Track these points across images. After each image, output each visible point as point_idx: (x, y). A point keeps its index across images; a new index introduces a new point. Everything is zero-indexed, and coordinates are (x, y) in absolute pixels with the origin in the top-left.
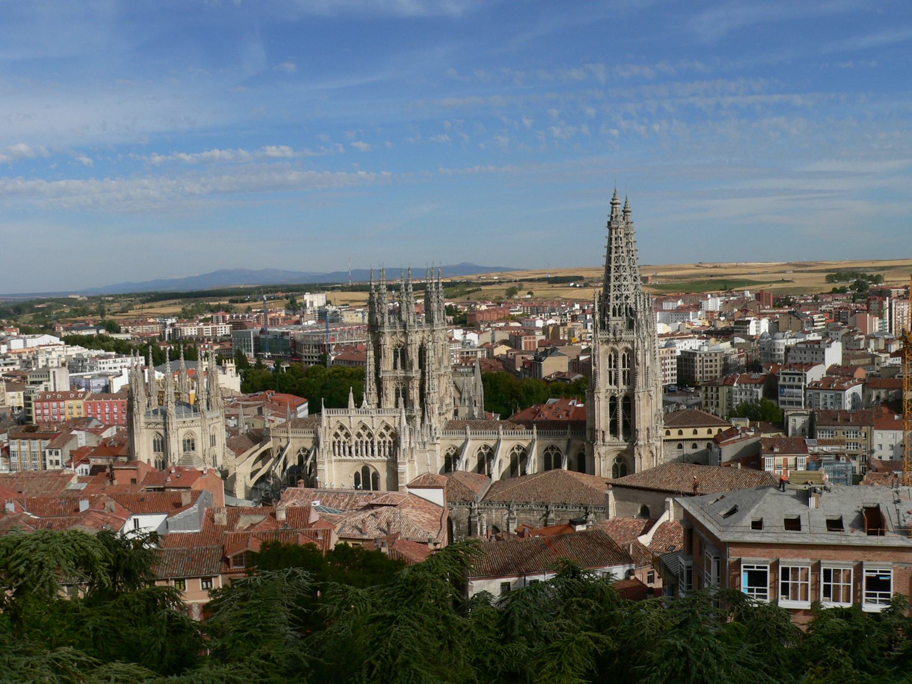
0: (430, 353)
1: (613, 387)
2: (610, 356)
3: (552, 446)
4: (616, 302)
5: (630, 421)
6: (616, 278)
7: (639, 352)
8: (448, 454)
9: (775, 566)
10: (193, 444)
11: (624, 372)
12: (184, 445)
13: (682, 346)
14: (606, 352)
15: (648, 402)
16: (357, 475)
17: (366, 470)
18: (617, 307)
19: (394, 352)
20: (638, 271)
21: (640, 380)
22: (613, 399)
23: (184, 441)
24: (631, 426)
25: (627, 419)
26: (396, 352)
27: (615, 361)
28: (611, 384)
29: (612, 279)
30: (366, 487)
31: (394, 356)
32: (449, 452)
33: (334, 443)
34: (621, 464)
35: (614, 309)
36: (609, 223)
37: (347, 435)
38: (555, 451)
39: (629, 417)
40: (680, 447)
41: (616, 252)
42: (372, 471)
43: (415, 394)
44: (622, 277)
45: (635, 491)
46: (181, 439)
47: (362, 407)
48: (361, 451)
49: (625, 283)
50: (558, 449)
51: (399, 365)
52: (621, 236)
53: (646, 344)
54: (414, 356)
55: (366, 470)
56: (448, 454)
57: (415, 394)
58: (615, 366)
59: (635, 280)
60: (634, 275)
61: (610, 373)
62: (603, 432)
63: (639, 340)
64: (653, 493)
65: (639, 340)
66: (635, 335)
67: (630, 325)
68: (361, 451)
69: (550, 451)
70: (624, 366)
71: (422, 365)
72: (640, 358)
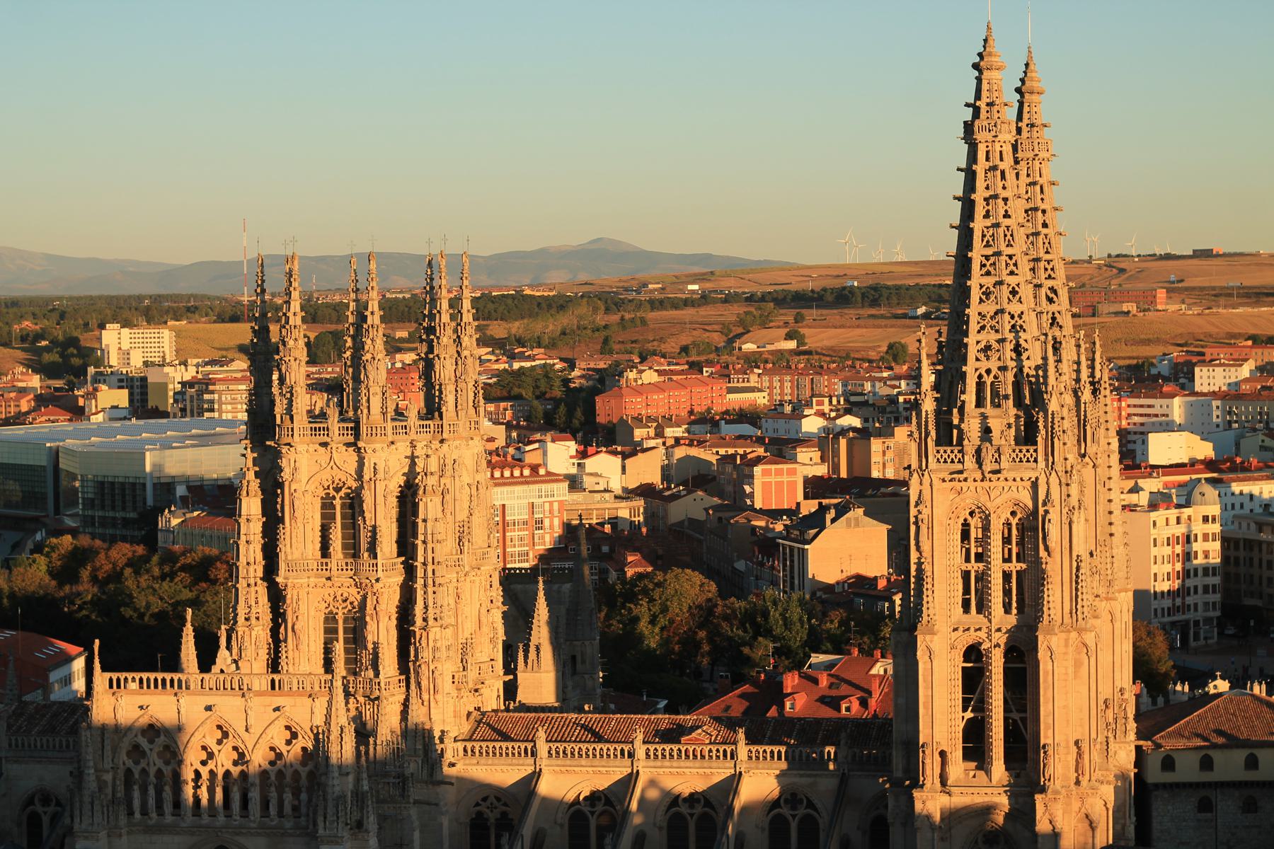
0: (429, 507)
1: (974, 617)
4: (984, 365)
5: (1024, 720)
6: (987, 294)
7: (1054, 515)
8: (480, 814)
11: (1007, 576)
13: (531, 501)
15: (1078, 664)
18: (988, 380)
19: (324, 506)
20: (1061, 273)
21: (1055, 597)
22: (973, 653)
24: (1028, 737)
25: (1016, 716)
26: (327, 505)
31: (323, 516)
32: (483, 808)
35: (980, 385)
36: (969, 128)
40: (1205, 806)
41: (987, 216)
43: (383, 632)
44: (1005, 291)
47: (215, 669)
49: (1015, 308)
52: (1002, 166)
53: (1074, 490)
57: (383, 632)
59: (1050, 300)
60: (1050, 283)
61: (966, 575)
62: (943, 754)
63: (1054, 479)
65: (1054, 479)
66: (1042, 464)
67: (1027, 436)
71: (406, 546)
72: (1054, 531)
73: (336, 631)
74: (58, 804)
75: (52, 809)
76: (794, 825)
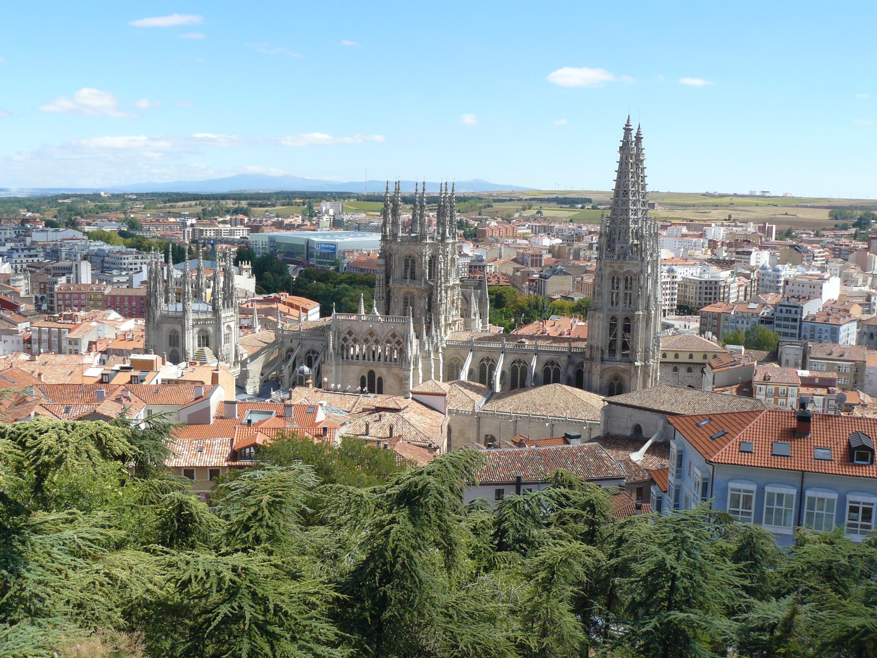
2: (613, 278)
9: (761, 491)
10: (207, 341)
11: (626, 294)
12: (199, 341)
14: (610, 274)
16: (363, 378)
17: (371, 374)
23: (199, 337)
25: (626, 340)
27: (618, 283)
28: (612, 305)
29: (620, 203)
30: (371, 391)
33: (343, 345)
38: (555, 367)
40: (675, 369)
42: (377, 377)
48: (368, 356)
50: (558, 365)
51: (408, 276)
55: (371, 374)
58: (618, 288)
64: (647, 412)
68: (368, 356)
70: (626, 288)
73: (407, 302)
74: (318, 354)
75: (315, 355)
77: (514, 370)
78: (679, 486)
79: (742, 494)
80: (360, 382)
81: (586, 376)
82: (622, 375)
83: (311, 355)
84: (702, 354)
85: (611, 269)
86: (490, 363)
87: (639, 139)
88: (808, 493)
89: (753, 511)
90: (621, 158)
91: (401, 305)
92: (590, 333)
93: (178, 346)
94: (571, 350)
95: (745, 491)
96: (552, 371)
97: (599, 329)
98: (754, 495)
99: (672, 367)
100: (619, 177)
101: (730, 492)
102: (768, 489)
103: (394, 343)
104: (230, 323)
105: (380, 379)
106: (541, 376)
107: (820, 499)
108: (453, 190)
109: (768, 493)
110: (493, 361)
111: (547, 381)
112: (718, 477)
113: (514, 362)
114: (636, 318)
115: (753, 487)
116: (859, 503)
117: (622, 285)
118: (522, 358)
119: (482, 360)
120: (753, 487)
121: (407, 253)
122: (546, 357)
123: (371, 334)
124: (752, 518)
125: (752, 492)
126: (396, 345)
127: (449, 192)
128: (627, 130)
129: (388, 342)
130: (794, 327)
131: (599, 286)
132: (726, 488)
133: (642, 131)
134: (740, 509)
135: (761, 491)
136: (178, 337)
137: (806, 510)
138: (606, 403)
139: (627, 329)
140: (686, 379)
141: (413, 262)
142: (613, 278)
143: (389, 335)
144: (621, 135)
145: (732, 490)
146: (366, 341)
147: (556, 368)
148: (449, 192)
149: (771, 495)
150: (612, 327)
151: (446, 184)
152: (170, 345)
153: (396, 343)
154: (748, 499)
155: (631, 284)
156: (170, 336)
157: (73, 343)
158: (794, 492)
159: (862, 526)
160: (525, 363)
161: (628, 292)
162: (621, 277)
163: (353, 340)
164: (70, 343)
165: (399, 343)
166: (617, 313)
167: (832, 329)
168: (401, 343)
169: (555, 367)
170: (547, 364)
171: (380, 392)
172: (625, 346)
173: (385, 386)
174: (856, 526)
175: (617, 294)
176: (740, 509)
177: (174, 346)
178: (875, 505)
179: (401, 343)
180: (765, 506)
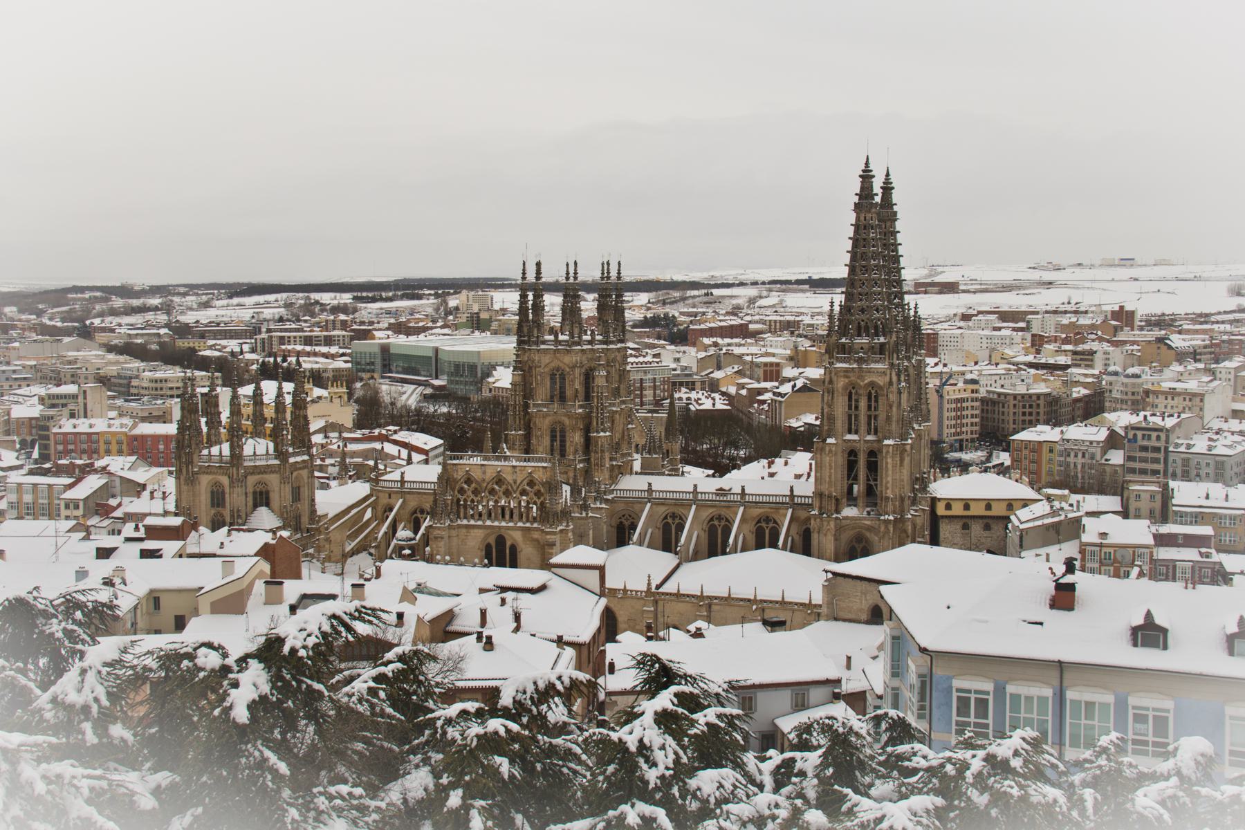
2: (850, 394)
3: (768, 517)
5: (876, 485)
8: (621, 523)
9: (1000, 691)
10: (268, 498)
11: (869, 417)
12: (255, 499)
14: (845, 388)
22: (852, 453)
23: (255, 493)
25: (872, 483)
26: (553, 376)
27: (857, 401)
32: (623, 520)
34: (861, 546)
37: (476, 492)
38: (771, 525)
39: (876, 480)
40: (965, 527)
42: (508, 544)
45: (864, 583)
46: (250, 490)
48: (496, 514)
54: (575, 384)
55: (501, 540)
56: (621, 523)
58: (857, 408)
61: (850, 417)
62: (837, 500)
69: (764, 525)
70: (869, 407)
76: (767, 532)
77: (712, 531)
78: (897, 689)
79: (973, 696)
80: (483, 553)
81: (815, 537)
82: (868, 534)
83: (419, 515)
84: (984, 503)
85: (847, 380)
86: (677, 521)
87: (887, 189)
88: (1070, 695)
89: (990, 721)
90: (858, 219)
91: (546, 441)
92: (818, 475)
93: (224, 506)
94: (793, 500)
95: (977, 692)
96: (767, 532)
97: (830, 469)
98: (991, 698)
99: (961, 523)
100: (855, 246)
101: (955, 695)
102: (1011, 689)
103: (532, 495)
104: (301, 472)
105: (514, 548)
106: (752, 539)
107: (1087, 703)
108: (619, 273)
109: (1011, 694)
110: (681, 518)
111: (760, 545)
112: (939, 672)
113: (712, 519)
114: (884, 451)
115: (988, 686)
116: (1147, 709)
117: (863, 404)
118: (723, 512)
119: (666, 518)
120: (988, 686)
121: (553, 365)
122: (756, 512)
123: (499, 480)
124: (990, 731)
125: (987, 693)
126: (535, 498)
127: (614, 274)
128: (866, 177)
129: (524, 492)
130: (1156, 461)
131: (829, 406)
132: (949, 689)
133: (893, 178)
134: (972, 719)
135: (1000, 691)
136: (223, 493)
137: (1068, 720)
138: (830, 575)
139: (873, 467)
140: (983, 540)
141: (563, 378)
142: (850, 394)
143: (525, 482)
144: (856, 186)
145: (958, 690)
146: (492, 492)
147: (773, 527)
148: (614, 274)
149: (1016, 698)
150: (851, 466)
151: (576, 263)
152: (213, 506)
153: (535, 494)
154: (982, 704)
155: (876, 401)
156: (212, 492)
157: (71, 506)
158: (1048, 692)
159: (1155, 744)
160: (727, 520)
161: (873, 413)
162: (862, 392)
163: (473, 492)
164: (67, 507)
165: (538, 494)
166: (858, 445)
167: (1183, 459)
168: (542, 495)
169: (771, 525)
170: (759, 522)
171: (514, 564)
172: (870, 492)
173: (521, 557)
174: (1145, 743)
175: (856, 416)
176: (972, 719)
177: (218, 506)
178: (1172, 712)
179: (542, 495)
180: (1008, 714)
